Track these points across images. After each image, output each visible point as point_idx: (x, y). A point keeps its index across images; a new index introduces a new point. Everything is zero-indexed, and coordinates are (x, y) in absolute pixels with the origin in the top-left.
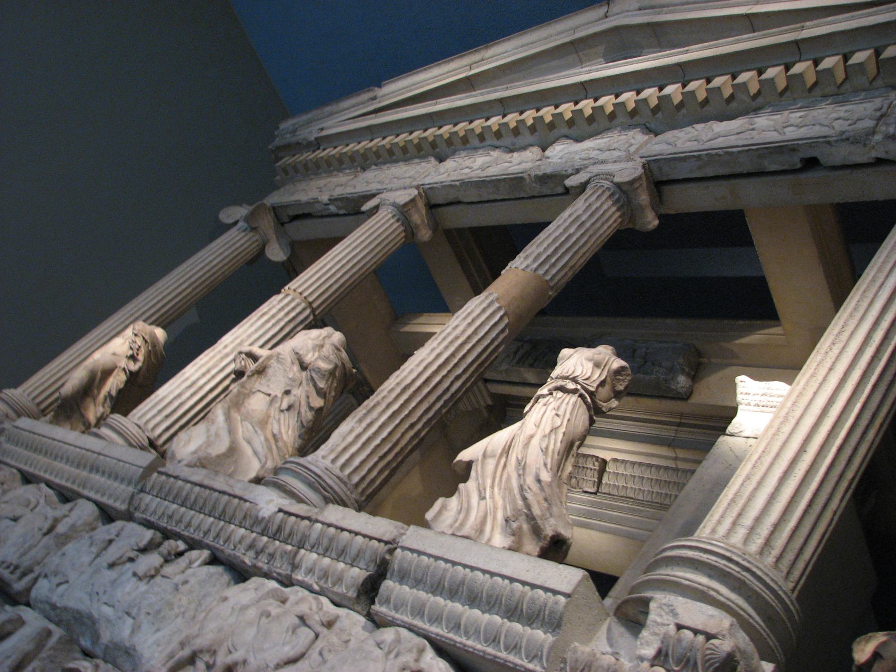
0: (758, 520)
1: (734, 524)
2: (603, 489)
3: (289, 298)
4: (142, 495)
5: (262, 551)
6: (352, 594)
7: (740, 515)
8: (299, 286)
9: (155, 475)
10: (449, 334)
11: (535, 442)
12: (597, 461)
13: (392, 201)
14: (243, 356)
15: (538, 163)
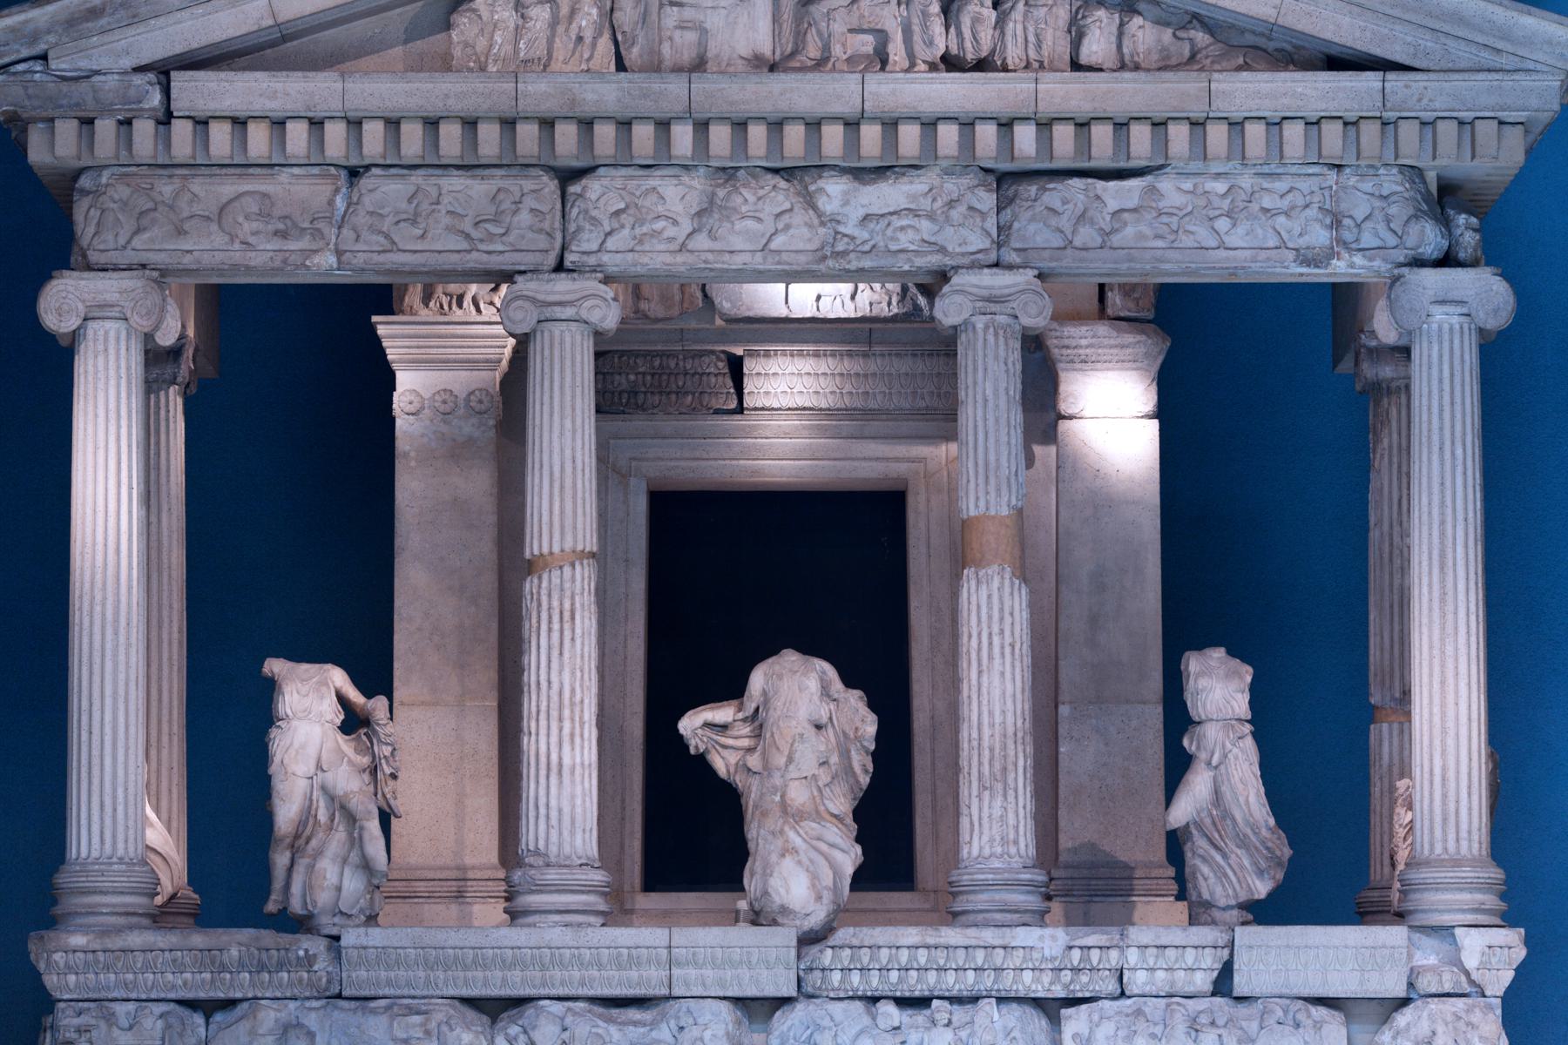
0: (1469, 832)
1: (1457, 840)
2: (748, 402)
3: (578, 567)
4: (818, 974)
5: (1072, 981)
6: (1209, 987)
7: (1457, 833)
8: (575, 537)
9: (829, 951)
10: (1002, 647)
11: (1252, 799)
12: (719, 359)
13: (569, 312)
14: (700, 732)
15: (822, 231)
